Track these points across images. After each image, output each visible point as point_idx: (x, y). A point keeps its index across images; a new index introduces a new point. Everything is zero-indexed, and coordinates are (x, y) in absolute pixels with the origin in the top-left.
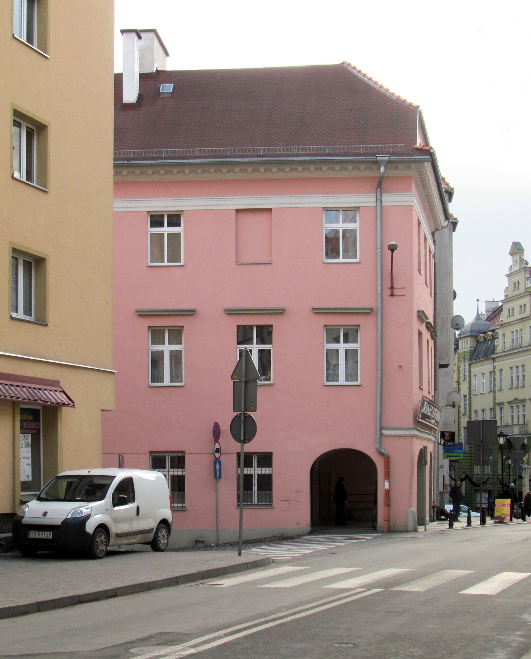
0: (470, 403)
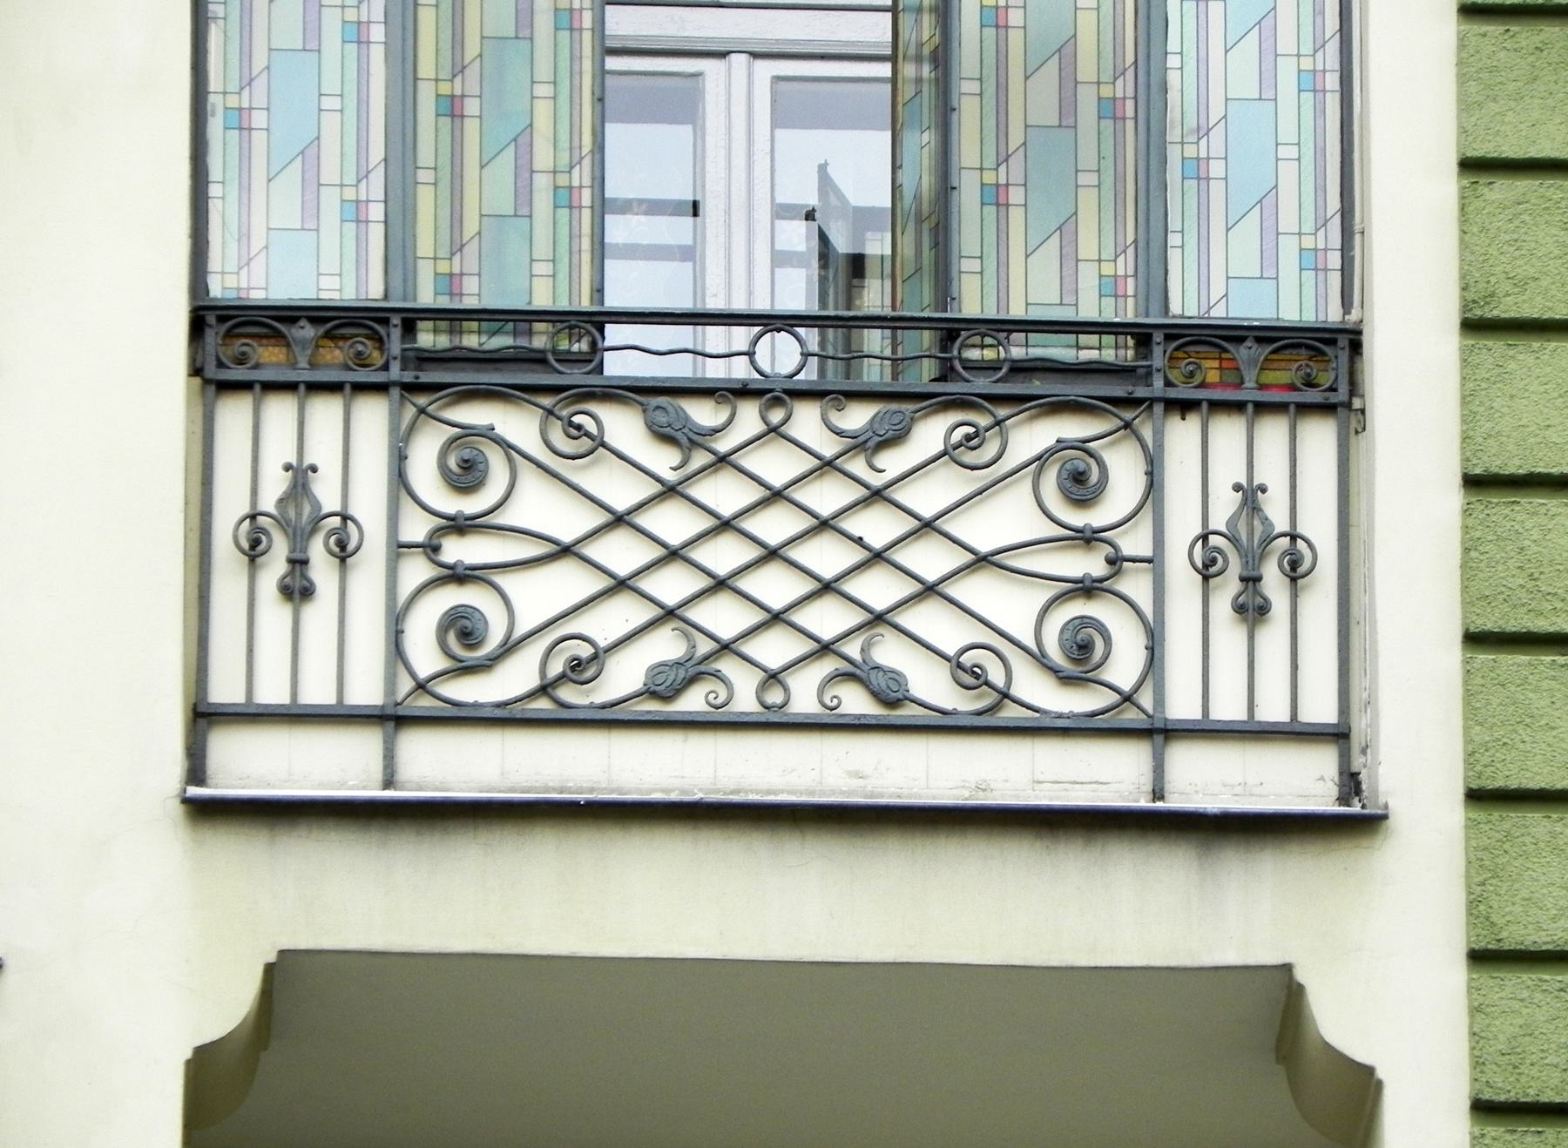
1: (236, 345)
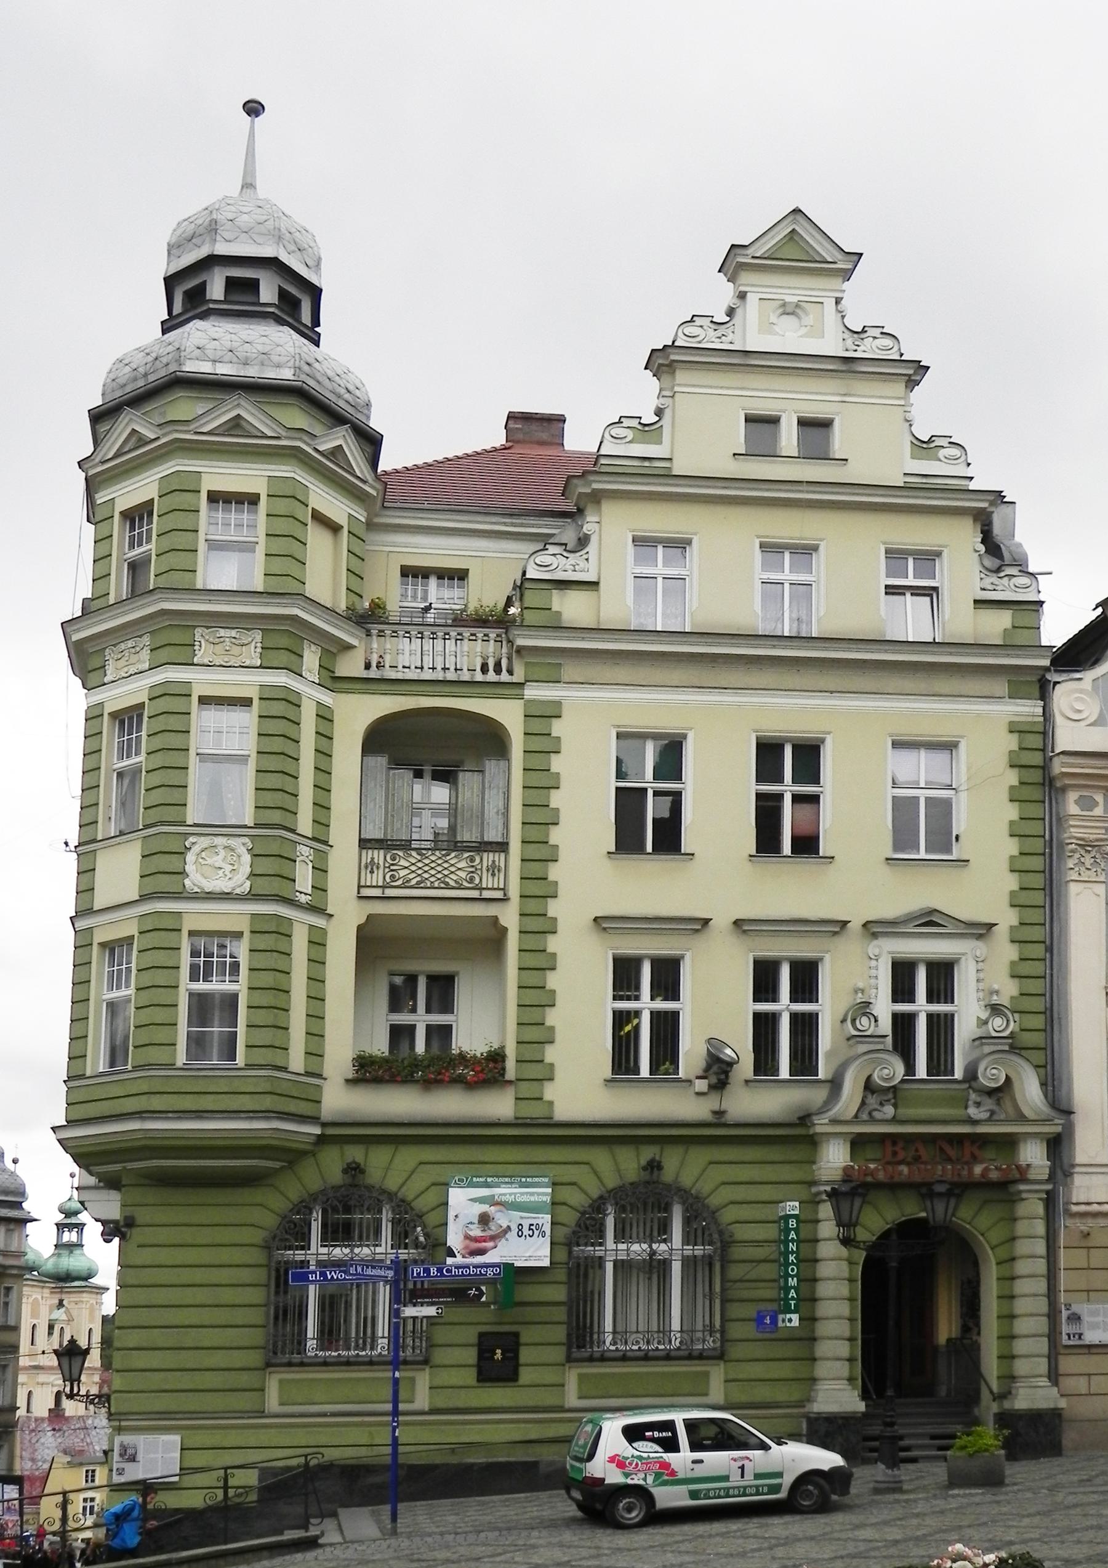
1: (364, 844)
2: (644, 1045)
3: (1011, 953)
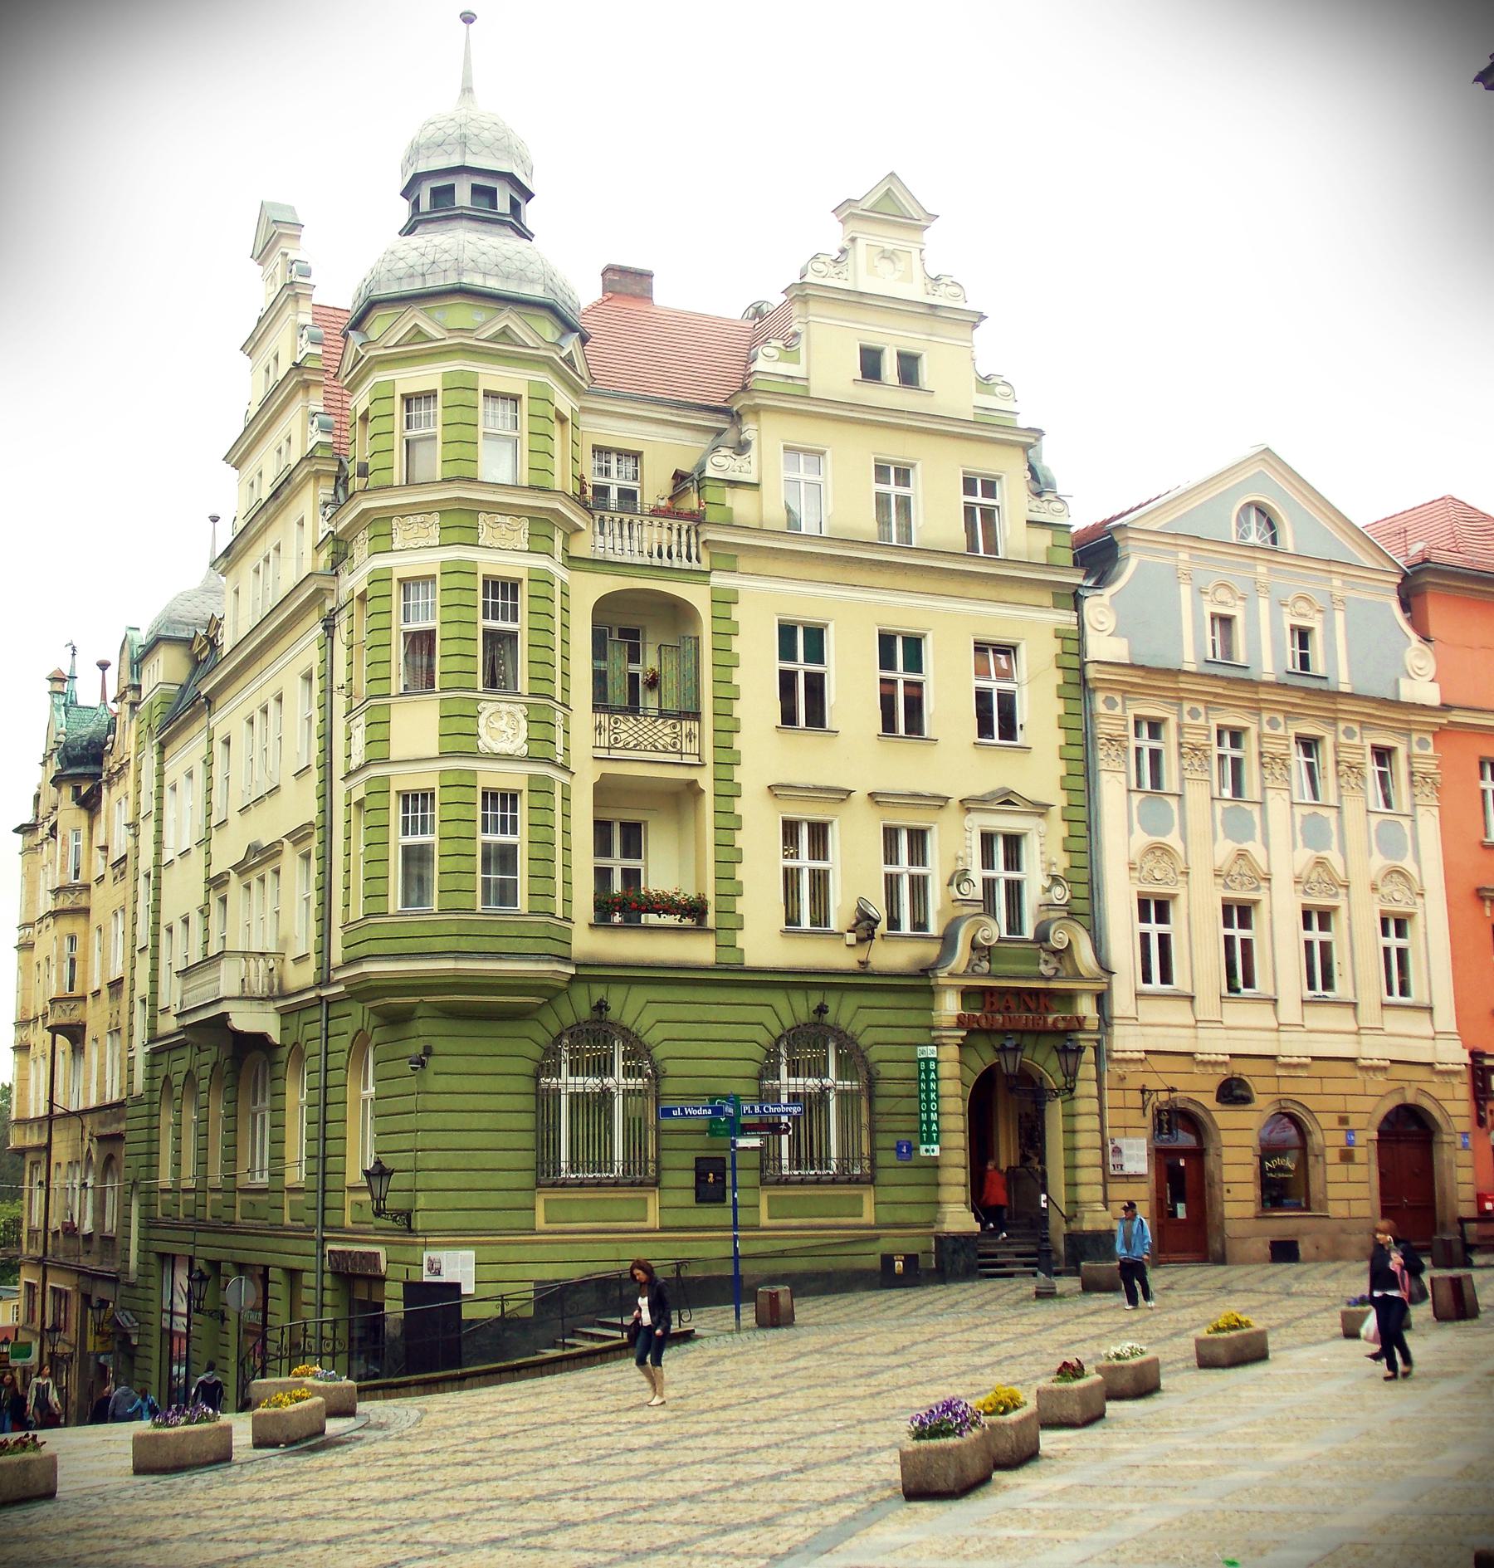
0: (157, 900)
2: (806, 898)
3: (1062, 830)
